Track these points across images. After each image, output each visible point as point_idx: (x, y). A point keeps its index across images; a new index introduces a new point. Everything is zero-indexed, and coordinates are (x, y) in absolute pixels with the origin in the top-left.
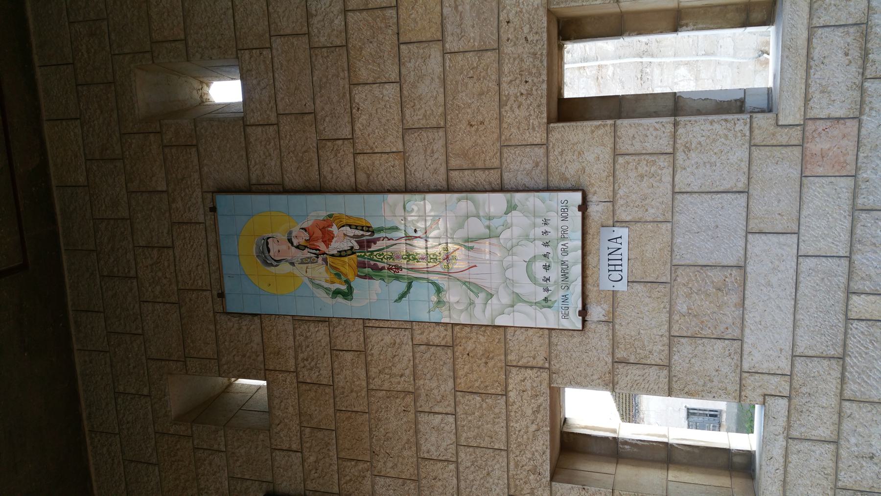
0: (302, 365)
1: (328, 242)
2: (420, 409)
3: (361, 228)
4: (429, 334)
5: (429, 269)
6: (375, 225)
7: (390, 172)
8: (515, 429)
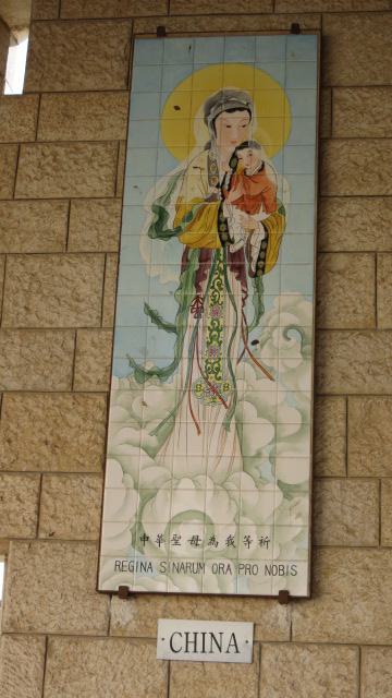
0: (47, 152)
4: (92, 355)
5: (195, 361)
6: (266, 279)
7: (346, 307)
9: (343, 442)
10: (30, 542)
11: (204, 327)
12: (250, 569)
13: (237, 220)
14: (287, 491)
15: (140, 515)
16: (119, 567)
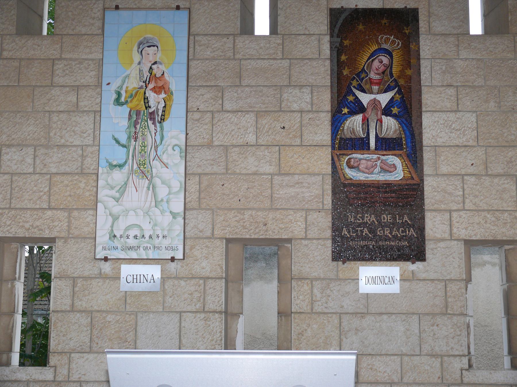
1: (154, 90)
2: (37, 148)
3: (163, 114)
6: (165, 124)
8: (25, 214)
9: (198, 194)
10: (66, 239)
11: (138, 145)
12: (159, 248)
13: (152, 96)
14: (174, 215)
15: (112, 226)
16: (104, 249)
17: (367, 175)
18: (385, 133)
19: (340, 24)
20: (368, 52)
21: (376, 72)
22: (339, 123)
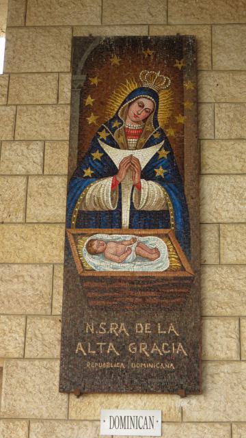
17: (117, 264)
18: (146, 202)
19: (86, 57)
20: (123, 92)
21: (134, 119)
22: (78, 190)
